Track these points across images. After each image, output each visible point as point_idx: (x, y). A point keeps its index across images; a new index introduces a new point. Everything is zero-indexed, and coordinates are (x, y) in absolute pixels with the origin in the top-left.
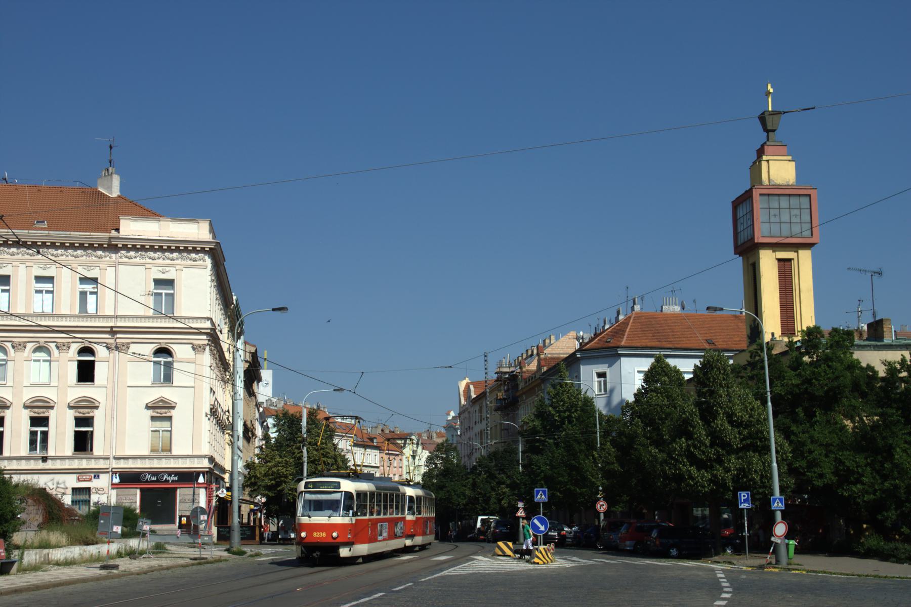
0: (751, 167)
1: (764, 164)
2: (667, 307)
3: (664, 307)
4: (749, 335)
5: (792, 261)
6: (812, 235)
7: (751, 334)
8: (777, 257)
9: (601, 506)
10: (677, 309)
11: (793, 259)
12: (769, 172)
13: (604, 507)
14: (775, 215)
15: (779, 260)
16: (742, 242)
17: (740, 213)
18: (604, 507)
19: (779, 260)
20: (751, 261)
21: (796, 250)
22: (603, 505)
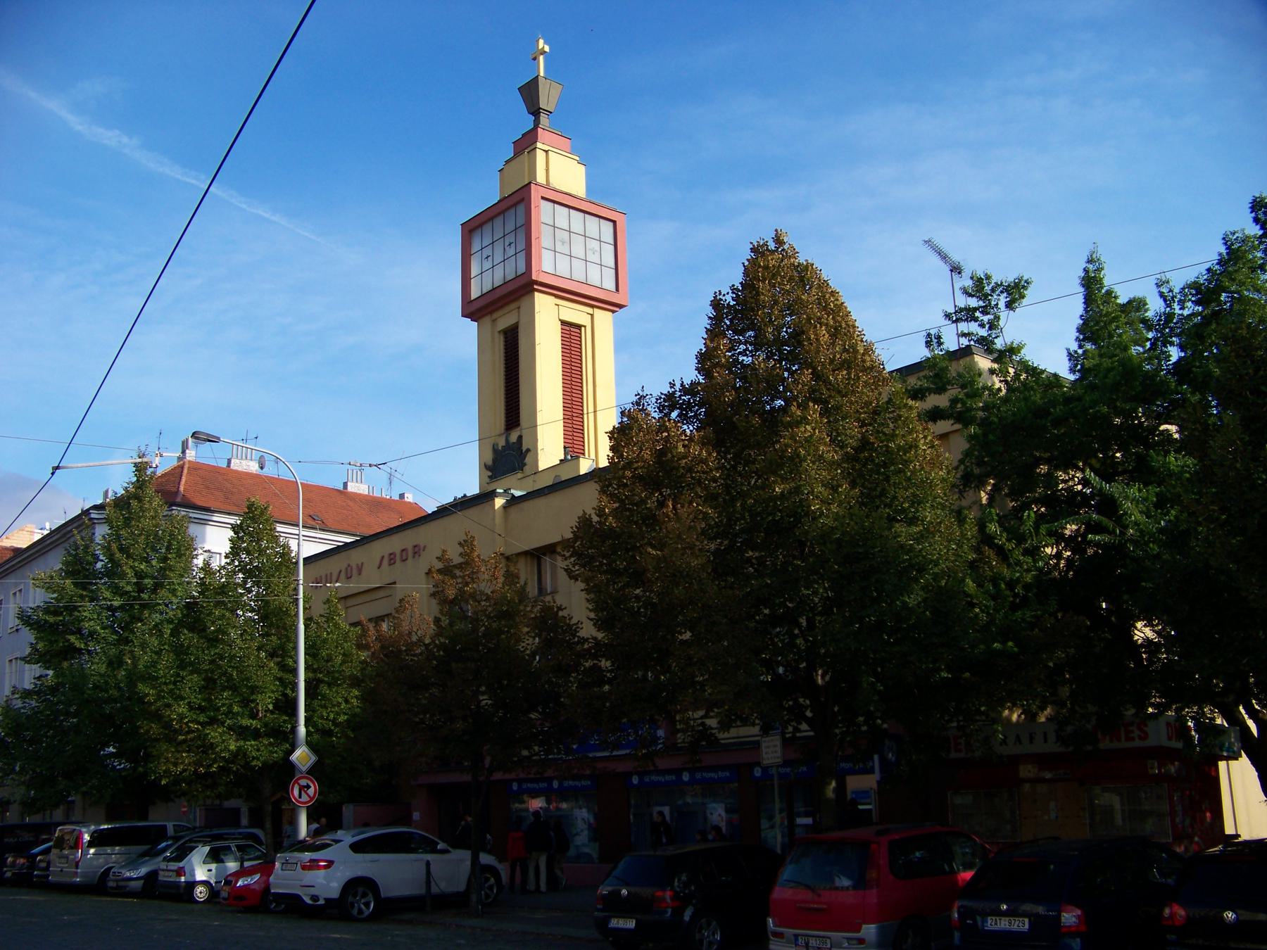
0: (507, 162)
1: (540, 156)
2: (238, 461)
3: (233, 461)
4: (490, 463)
5: (583, 329)
6: (617, 289)
7: (494, 461)
8: (561, 318)
9: (301, 788)
10: (253, 467)
11: (585, 327)
12: (547, 171)
13: (311, 791)
14: (563, 243)
15: (563, 323)
16: (487, 287)
17: (476, 246)
18: (311, 791)
19: (563, 323)
20: (505, 321)
21: (590, 310)
22: (308, 787)
